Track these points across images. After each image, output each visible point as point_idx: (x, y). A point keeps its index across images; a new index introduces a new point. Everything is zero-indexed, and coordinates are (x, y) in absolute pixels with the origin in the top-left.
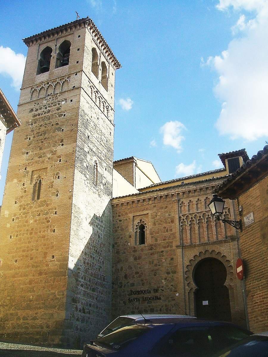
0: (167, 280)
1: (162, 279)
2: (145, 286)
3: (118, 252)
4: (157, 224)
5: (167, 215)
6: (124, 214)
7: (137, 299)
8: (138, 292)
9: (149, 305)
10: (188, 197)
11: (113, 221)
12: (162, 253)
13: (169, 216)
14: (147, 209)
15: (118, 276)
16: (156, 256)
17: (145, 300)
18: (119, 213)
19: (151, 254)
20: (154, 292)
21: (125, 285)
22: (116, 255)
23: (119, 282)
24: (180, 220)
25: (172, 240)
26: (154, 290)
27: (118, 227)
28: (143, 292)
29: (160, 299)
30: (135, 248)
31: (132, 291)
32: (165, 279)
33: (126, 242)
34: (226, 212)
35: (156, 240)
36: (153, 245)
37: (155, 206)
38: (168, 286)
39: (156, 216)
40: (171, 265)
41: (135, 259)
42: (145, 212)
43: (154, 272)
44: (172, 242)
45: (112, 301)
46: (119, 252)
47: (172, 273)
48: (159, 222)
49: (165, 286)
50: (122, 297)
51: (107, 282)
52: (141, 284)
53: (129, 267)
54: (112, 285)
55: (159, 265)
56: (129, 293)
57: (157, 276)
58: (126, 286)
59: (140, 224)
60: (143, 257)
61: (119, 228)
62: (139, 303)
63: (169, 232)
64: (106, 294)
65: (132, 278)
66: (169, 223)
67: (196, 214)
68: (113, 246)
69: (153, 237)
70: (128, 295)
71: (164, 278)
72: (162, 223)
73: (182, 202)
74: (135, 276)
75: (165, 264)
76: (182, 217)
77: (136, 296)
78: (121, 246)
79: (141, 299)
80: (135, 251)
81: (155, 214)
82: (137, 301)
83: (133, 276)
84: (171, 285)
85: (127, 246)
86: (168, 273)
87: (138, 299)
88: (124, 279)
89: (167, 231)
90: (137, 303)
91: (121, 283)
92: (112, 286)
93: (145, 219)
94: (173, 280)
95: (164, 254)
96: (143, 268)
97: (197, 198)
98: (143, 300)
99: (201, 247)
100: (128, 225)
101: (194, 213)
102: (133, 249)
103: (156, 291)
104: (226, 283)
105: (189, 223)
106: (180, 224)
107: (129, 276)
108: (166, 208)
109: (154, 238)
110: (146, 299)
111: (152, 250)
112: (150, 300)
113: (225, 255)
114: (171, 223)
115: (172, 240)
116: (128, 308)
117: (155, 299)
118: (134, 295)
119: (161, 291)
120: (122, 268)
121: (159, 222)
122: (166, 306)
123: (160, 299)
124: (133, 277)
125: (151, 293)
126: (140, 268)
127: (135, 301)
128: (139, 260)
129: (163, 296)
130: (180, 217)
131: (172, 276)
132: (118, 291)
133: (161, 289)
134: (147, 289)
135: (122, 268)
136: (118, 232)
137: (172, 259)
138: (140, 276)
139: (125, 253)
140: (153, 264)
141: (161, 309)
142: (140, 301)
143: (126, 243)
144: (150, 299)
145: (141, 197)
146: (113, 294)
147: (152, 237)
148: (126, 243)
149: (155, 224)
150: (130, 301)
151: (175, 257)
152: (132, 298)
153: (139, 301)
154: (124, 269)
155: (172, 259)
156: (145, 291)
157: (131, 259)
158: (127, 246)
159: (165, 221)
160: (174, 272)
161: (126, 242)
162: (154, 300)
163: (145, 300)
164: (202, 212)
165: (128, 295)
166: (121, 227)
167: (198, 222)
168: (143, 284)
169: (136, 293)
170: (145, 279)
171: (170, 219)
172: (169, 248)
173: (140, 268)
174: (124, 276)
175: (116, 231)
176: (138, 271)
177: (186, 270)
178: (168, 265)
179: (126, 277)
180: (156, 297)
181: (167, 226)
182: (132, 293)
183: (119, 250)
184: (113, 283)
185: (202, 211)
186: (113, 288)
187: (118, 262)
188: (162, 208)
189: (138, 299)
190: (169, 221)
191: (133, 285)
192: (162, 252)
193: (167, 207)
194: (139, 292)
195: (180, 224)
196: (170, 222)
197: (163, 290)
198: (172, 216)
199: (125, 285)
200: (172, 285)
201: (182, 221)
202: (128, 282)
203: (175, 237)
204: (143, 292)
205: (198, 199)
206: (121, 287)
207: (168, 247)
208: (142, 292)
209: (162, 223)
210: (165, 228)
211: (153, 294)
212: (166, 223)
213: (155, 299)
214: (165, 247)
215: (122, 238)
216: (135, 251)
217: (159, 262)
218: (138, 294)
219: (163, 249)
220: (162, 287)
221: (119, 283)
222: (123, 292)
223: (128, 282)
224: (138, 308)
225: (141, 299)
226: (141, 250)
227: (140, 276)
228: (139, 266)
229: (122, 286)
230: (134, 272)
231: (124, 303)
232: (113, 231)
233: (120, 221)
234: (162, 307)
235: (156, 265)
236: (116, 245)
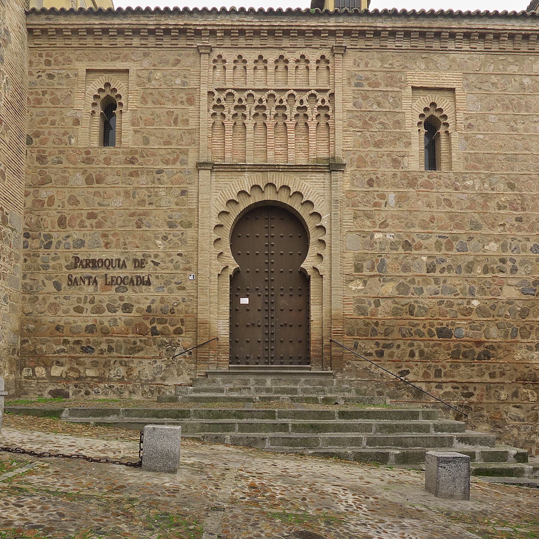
0: (169, 242)
1: (156, 238)
2: (110, 250)
3: (41, 159)
4: (149, 99)
5: (178, 81)
6: (61, 59)
7: (89, 278)
8: (94, 261)
9: (120, 294)
10: (235, 47)
11: (30, 73)
12: (158, 175)
13: (184, 86)
14: (126, 58)
15: (42, 219)
16: (143, 180)
17: (111, 284)
18: (47, 55)
19: (131, 175)
20: (135, 267)
21: (59, 243)
22: (37, 164)
23: (43, 233)
24: (209, 103)
25: (188, 147)
26: (135, 261)
27: (44, 93)
28: (107, 263)
29: (149, 283)
30: (88, 153)
31: (77, 259)
32: (165, 238)
33: (64, 134)
34: (323, 101)
35: (146, 141)
36: (136, 152)
37: (146, 55)
38: (169, 255)
39: (149, 80)
40: (179, 207)
41: (89, 181)
42: (120, 65)
43: (136, 218)
44: (185, 152)
45: (24, 277)
46: (45, 157)
47: (182, 226)
48: (157, 97)
49: (162, 255)
50: (50, 270)
51: (11, 228)
52: (103, 244)
53: (69, 198)
54: (23, 239)
55: (150, 204)
56: (69, 263)
57: (144, 228)
58: (62, 245)
59: (103, 95)
60: (109, 179)
61: (47, 96)
62: (96, 290)
63: (180, 126)
64: (10, 260)
65: (77, 228)
66: (182, 103)
67: (251, 91)
68: (29, 141)
69: (139, 132)
70: (67, 267)
71: (160, 236)
72: (164, 100)
73: (220, 56)
74: (88, 223)
75: (163, 203)
76: (216, 93)
77: (88, 272)
78: (50, 144)
79: (100, 281)
80: (88, 161)
81: (145, 74)
82: (89, 284)
83: (82, 221)
84: (180, 255)
85: (66, 144)
86: (171, 225)
87: (92, 280)
88: (57, 228)
89: (176, 122)
90: (91, 288)
91: (48, 237)
92: (24, 242)
93: (118, 83)
94: (184, 242)
95: (164, 177)
96: (109, 205)
97: (258, 52)
98: (106, 284)
99: (257, 173)
100: (71, 91)
101: (246, 90)
102: (84, 156)
103: (139, 264)
104: (307, 265)
105: (233, 112)
106: (209, 111)
107: (70, 219)
108: (175, 65)
109: (138, 135)
110: (113, 281)
111: (133, 163)
112: (122, 285)
113: (310, 199)
114: (185, 103)
115: (188, 147)
116: (65, 298)
117: (135, 283)
118: (83, 267)
119: (152, 264)
120: (51, 200)
121: (157, 97)
122: (162, 301)
123: (149, 283)
124: (82, 225)
125: (126, 267)
126: (100, 204)
127: (84, 283)
128: (98, 185)
129: (157, 277)
130: (211, 93)
131: (181, 232)
132: (41, 255)
133: (152, 261)
134: (116, 257)
135: (51, 200)
136: (43, 105)
137: (184, 192)
138: (99, 225)
139: (60, 162)
140: (134, 198)
141: (149, 307)
142: (97, 284)
143: (66, 138)
144: (123, 281)
145: (112, 22)
146: (25, 260)
147: (136, 132)
148: (66, 138)
149: (144, 100)
150: (73, 282)
151: (192, 189)
152: (78, 276)
153: (95, 284)
154: (56, 203)
155: (184, 192)
156: (111, 262)
157: (79, 179)
158: (66, 144)
159: (171, 96)
160: (190, 225)
161: (64, 134)
162: (134, 285)
163: (109, 283)
164: (269, 90)
165: (67, 267)
166: (52, 94)
167: (254, 112)
168: (107, 245)
169: (87, 265)
170: (112, 232)
171: (186, 94)
172: (178, 166)
173: (100, 204)
174: (56, 220)
175: (39, 102)
176: (95, 211)
177: (215, 221)
178: (175, 207)
179: (62, 222)
180: (138, 277)
181: (178, 109)
182: (77, 262)
183: (44, 152)
184: (27, 235)
185: (268, 88)
186: (26, 247)
187: (43, 183)
188: (167, 62)
189: (92, 280)
190: (182, 98)
191: (81, 243)
192: (160, 172)
193: (178, 62)
194: (94, 264)
195: (209, 111)
196: (184, 99)
197: (156, 264)
198: (191, 87)
199: (59, 243)
200: (180, 255)
201: (215, 102)
202: (68, 237)
203: (195, 142)
204: (107, 263)
205: (261, 57)
206: (48, 246)
207: (174, 161)
208: (103, 262)
209: (164, 100)
210: (170, 113)
211: (129, 272)
212: (174, 101)
213: (135, 283)
214: (167, 162)
215: (53, 123)
216: (88, 161)
217: (149, 196)
218: (94, 267)
219: (161, 166)
220: (156, 256)
221: (42, 235)
222: (54, 259)
223: (68, 237)
224: (92, 302)
225: (100, 281)
226: (104, 159)
227: (99, 225)
228: (97, 199)
229: (51, 243)
230: (85, 213)
231: (57, 286)
232: (28, 99)
233: (51, 76)
234: (153, 301)
235: (142, 202)
236: (37, 139)
